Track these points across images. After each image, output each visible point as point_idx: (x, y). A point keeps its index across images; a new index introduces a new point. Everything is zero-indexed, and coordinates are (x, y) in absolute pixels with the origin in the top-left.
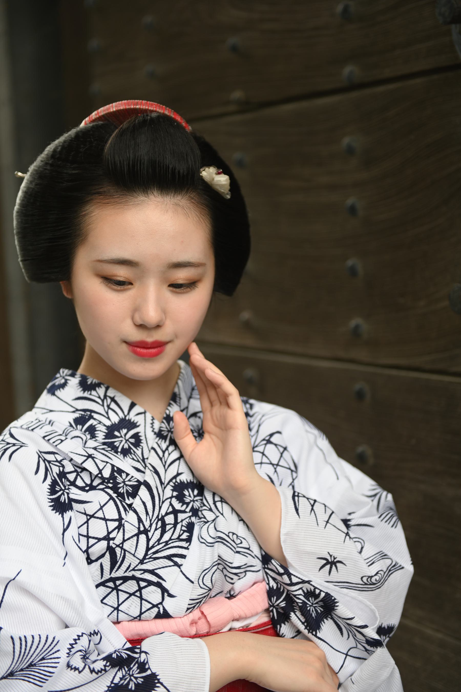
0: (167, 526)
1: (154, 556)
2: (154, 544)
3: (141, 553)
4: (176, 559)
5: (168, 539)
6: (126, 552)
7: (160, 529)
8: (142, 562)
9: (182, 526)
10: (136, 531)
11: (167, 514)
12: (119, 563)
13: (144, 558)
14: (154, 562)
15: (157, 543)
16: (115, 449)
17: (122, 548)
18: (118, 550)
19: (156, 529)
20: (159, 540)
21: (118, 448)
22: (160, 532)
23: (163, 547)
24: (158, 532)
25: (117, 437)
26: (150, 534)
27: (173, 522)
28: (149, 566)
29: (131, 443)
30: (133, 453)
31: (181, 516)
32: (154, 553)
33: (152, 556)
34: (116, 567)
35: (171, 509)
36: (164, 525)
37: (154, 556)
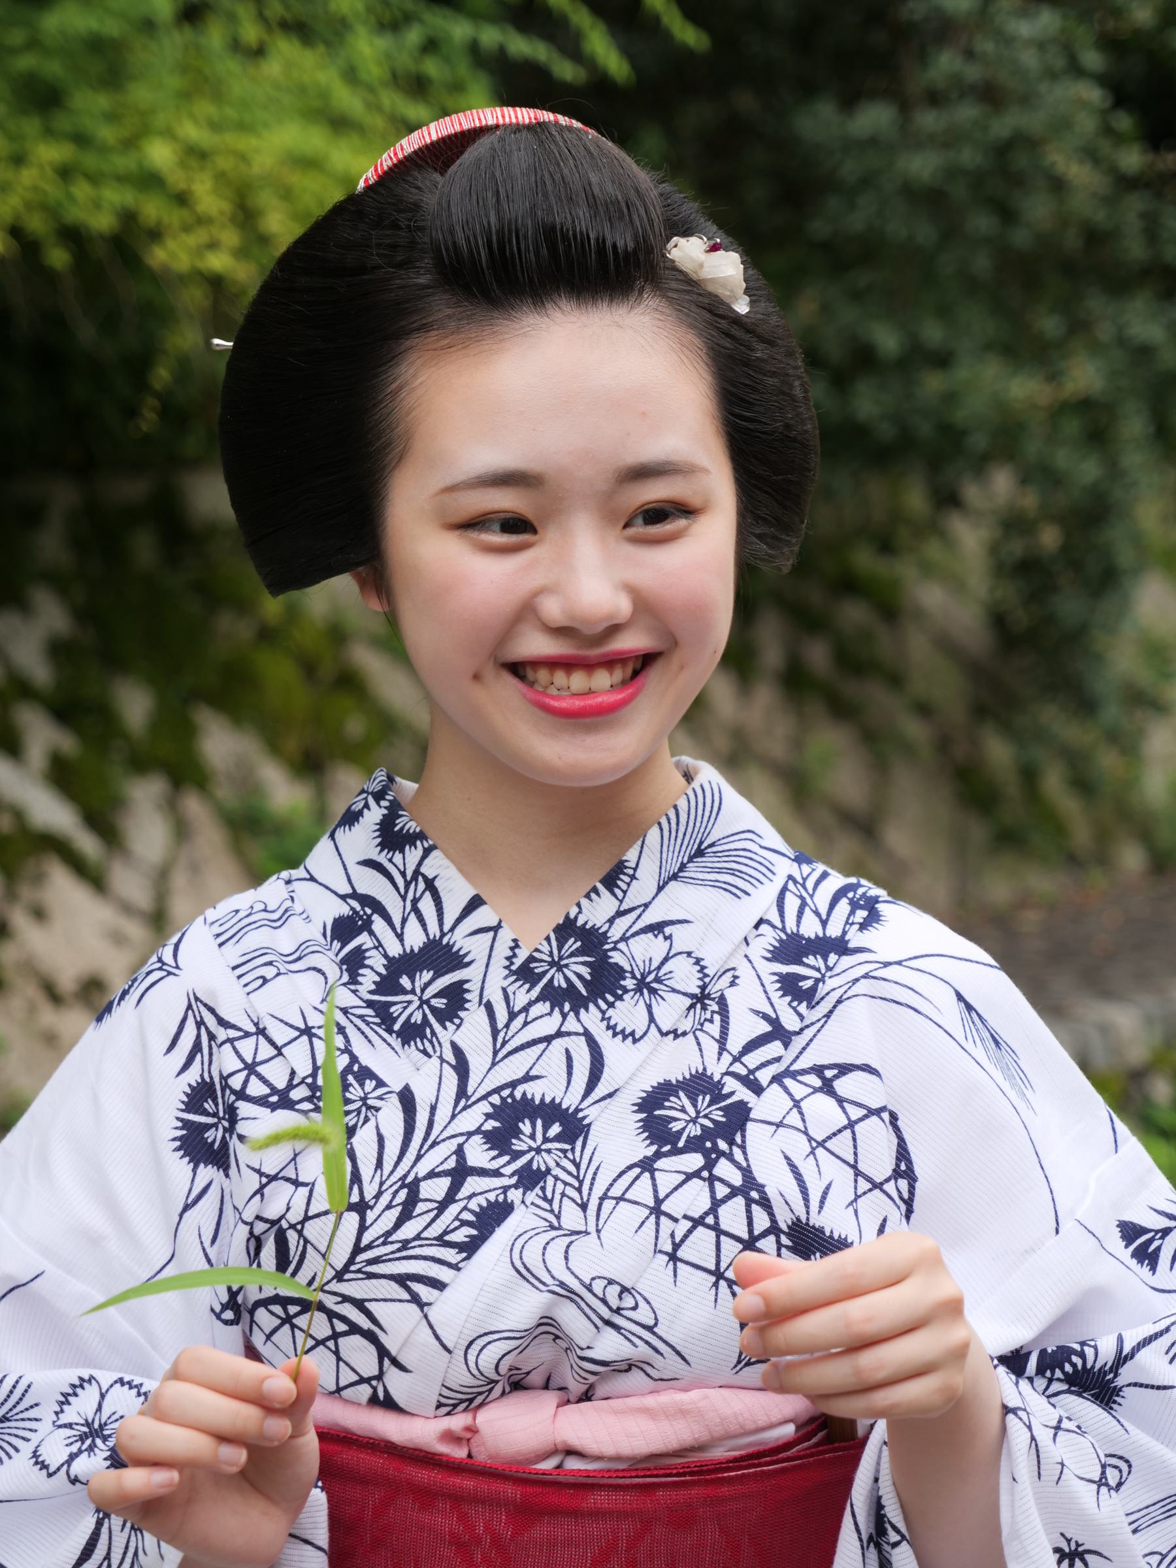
0: (420, 1204)
1: (369, 1269)
2: (373, 1241)
3: (339, 1257)
4: (417, 1287)
5: (411, 1236)
7: (399, 1208)
8: (339, 1276)
13: (346, 1269)
14: (366, 1281)
15: (382, 1240)
16: (387, 1020)
17: (300, 1233)
18: (292, 1236)
19: (389, 1207)
20: (388, 1234)
21: (395, 1019)
22: (397, 1215)
23: (393, 1253)
24: (395, 1213)
25: (404, 992)
26: (370, 1216)
29: (434, 1010)
30: (429, 1036)
32: (371, 1262)
36: (413, 1199)
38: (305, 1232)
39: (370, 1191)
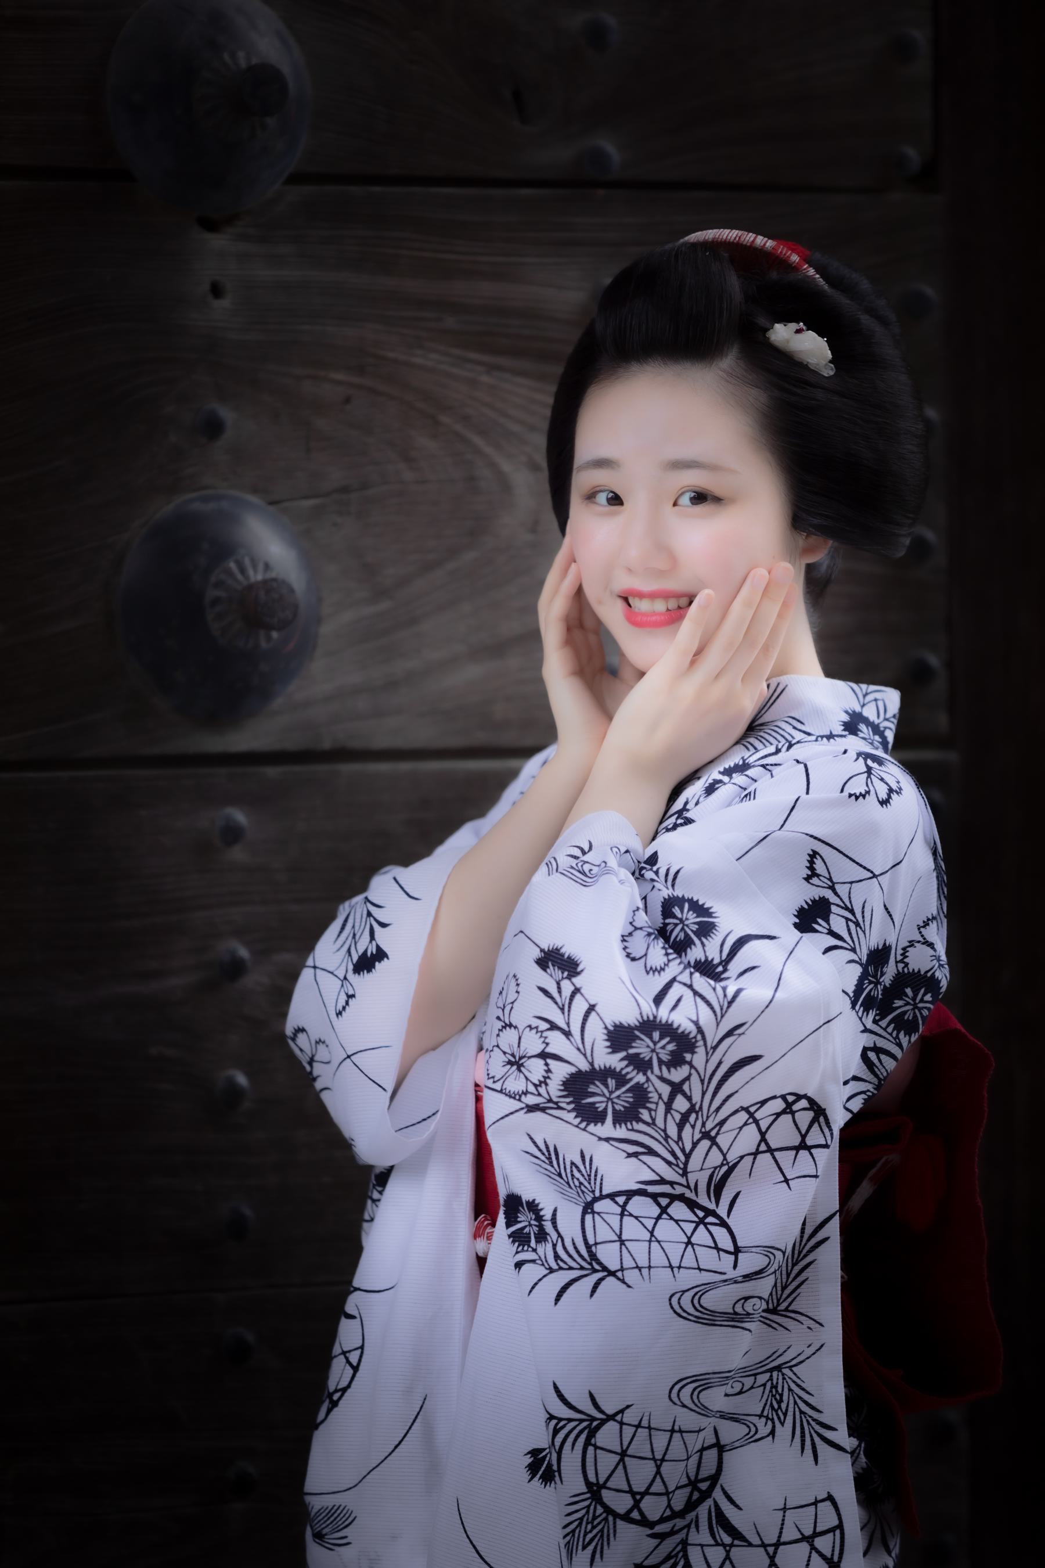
1: (672, 1561)
6: (712, 1542)
8: (685, 1543)
12: (714, 1522)
13: (684, 1550)
17: (724, 1545)
18: (727, 1540)
33: (676, 1560)
34: (713, 1514)
37: (672, 1561)
38: (721, 1548)
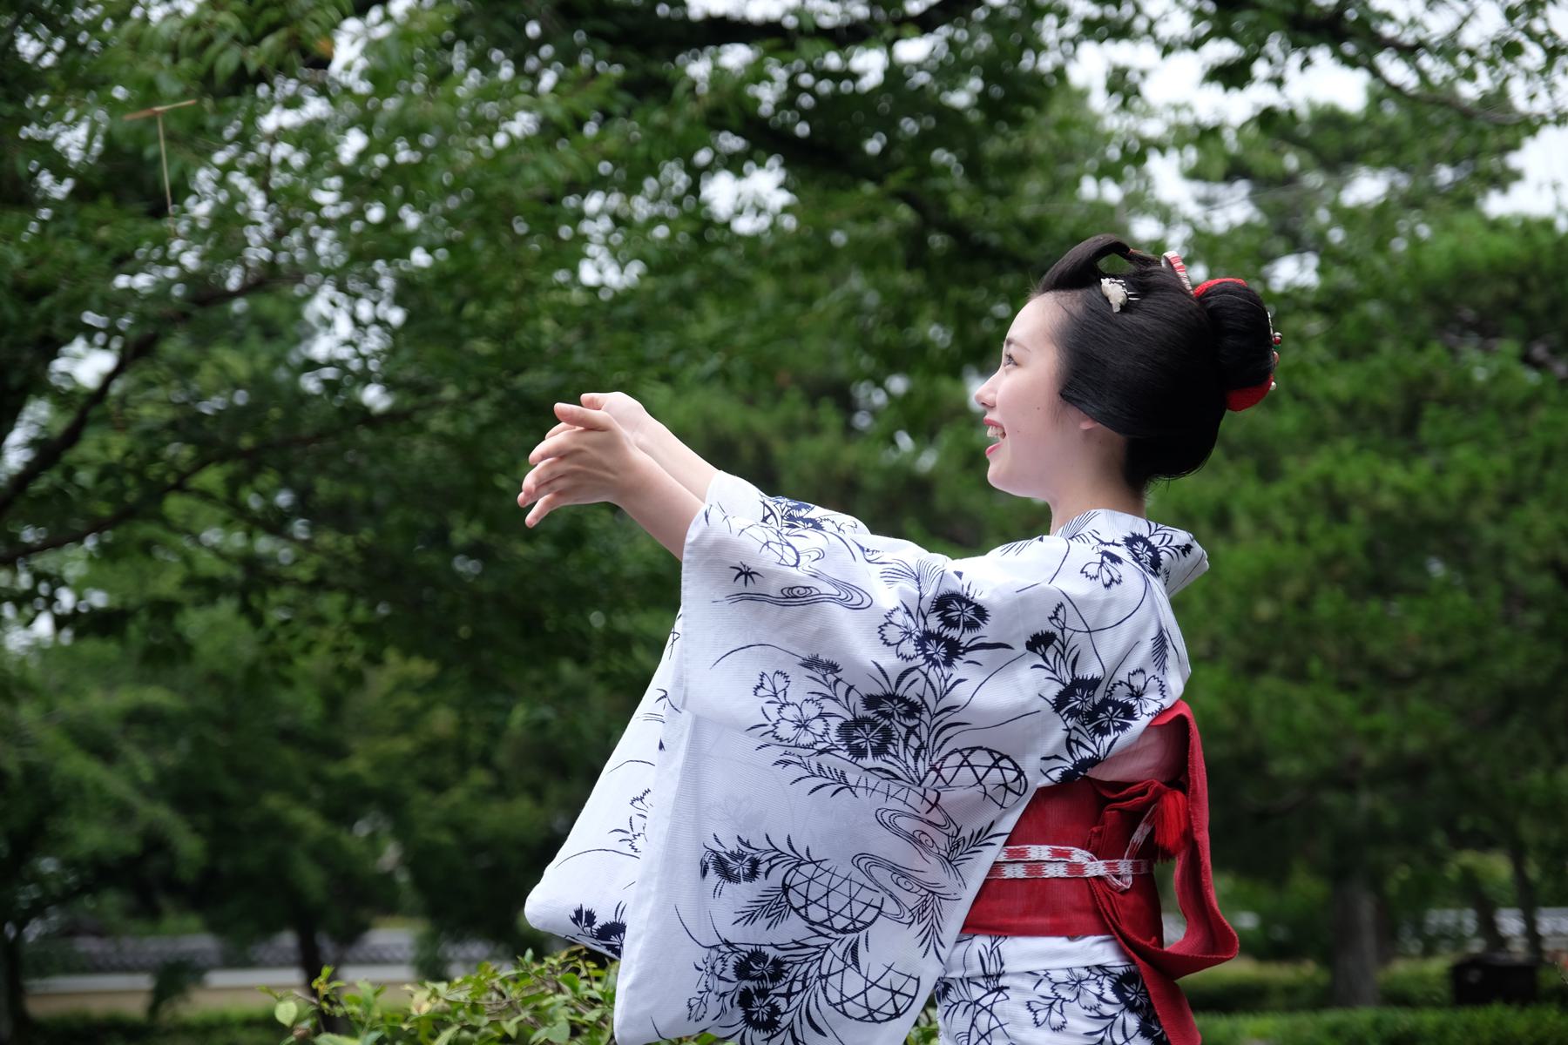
1: (817, 950)
3: (829, 955)
8: (829, 946)
9: (787, 978)
10: (830, 979)
11: (798, 993)
13: (826, 949)
19: (811, 977)
20: (811, 966)
26: (817, 973)
27: (795, 983)
28: (822, 941)
31: (784, 990)
32: (815, 953)
35: (792, 998)
36: (804, 982)
37: (817, 950)
39: (818, 983)
